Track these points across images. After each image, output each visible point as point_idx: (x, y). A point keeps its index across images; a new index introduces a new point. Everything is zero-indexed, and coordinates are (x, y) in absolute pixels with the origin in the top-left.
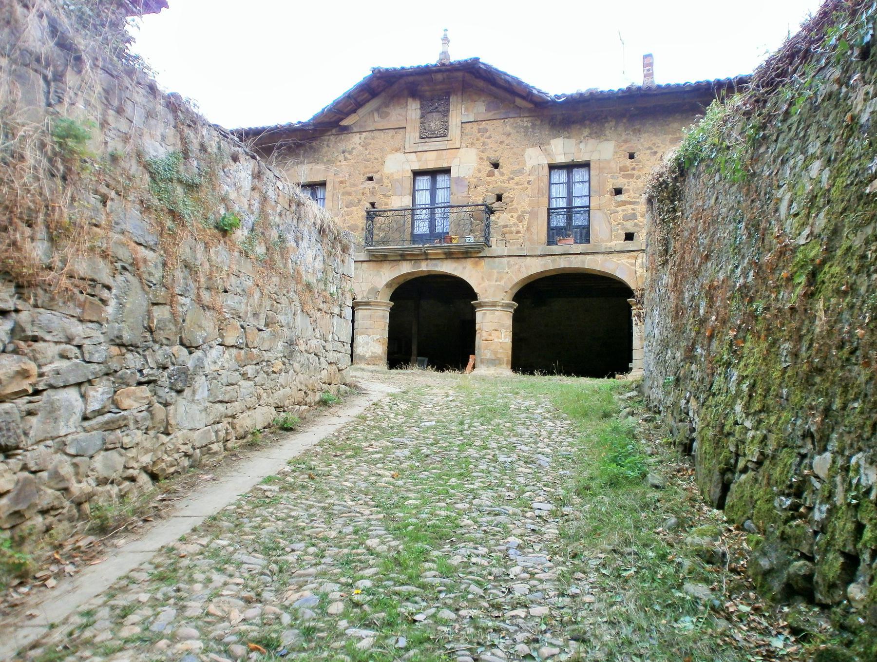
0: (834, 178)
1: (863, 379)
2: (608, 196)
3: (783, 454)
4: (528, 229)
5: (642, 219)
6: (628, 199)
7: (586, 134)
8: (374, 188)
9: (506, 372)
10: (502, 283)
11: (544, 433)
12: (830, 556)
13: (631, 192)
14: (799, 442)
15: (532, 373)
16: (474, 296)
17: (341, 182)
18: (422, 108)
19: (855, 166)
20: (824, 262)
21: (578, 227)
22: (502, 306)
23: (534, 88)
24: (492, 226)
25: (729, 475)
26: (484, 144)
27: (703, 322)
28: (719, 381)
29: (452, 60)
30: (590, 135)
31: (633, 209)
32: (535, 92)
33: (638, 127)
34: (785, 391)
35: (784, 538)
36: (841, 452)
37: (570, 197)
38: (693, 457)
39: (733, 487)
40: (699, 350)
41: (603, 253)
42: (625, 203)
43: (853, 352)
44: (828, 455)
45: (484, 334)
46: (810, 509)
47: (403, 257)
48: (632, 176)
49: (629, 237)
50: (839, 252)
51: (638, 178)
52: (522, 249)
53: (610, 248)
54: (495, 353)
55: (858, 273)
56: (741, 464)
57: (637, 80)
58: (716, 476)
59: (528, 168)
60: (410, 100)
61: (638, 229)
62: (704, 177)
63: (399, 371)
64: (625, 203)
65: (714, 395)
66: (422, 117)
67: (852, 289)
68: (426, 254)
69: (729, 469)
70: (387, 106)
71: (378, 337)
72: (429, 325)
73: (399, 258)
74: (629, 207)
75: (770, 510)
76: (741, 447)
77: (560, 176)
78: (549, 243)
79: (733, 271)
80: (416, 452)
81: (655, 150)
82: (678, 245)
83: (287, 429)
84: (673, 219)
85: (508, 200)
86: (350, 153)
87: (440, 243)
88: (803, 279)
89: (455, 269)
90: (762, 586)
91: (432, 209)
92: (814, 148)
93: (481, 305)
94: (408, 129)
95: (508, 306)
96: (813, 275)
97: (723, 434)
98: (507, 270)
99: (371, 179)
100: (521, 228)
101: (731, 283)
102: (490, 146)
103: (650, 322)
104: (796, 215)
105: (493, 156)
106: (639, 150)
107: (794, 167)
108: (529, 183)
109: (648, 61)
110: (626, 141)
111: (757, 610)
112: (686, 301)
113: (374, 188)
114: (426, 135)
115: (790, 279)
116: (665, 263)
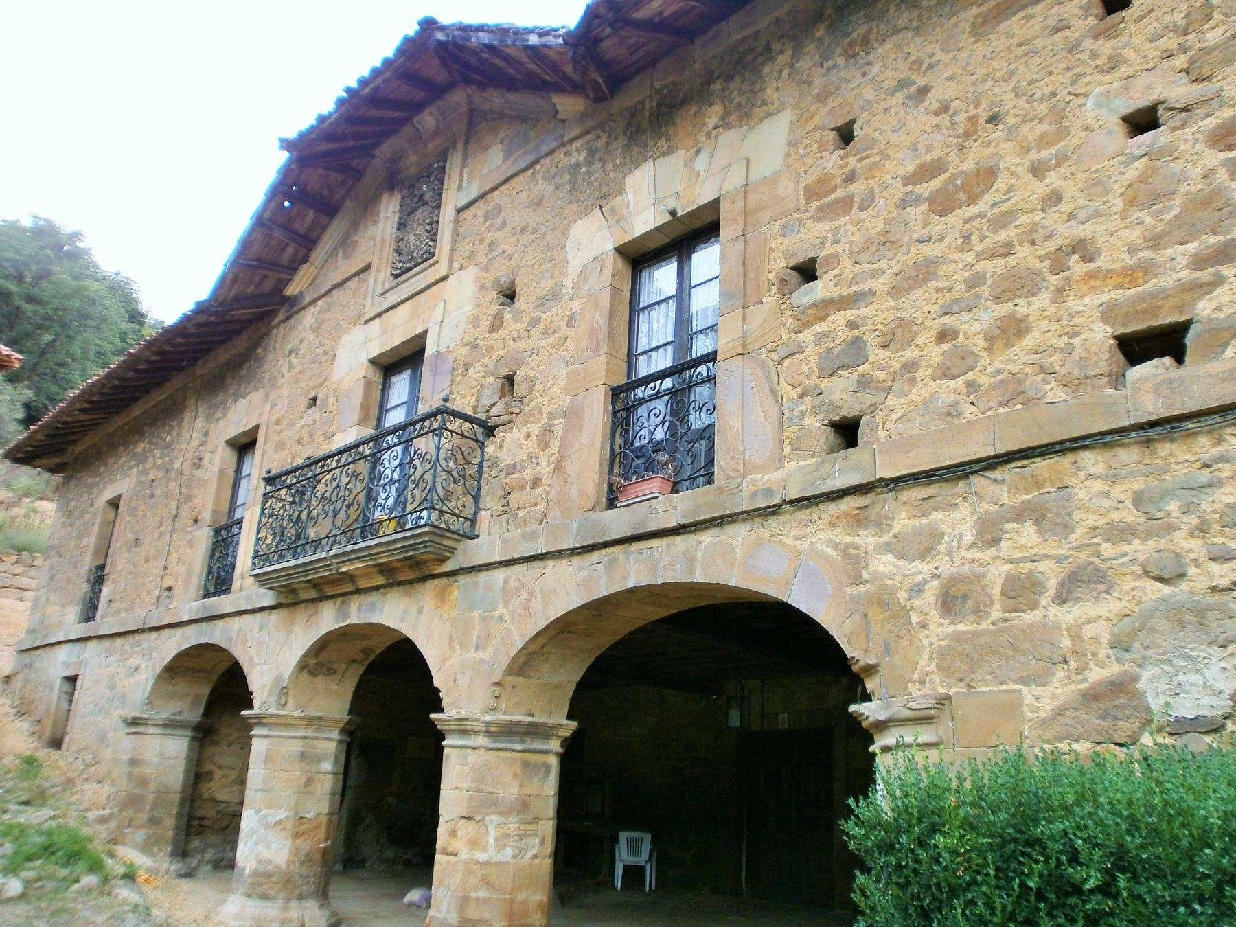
4: (559, 467)
5: (883, 355)
6: (835, 293)
7: (712, 121)
10: (487, 655)
13: (845, 262)
30: (725, 123)
31: (853, 325)
41: (748, 515)
42: (824, 309)
48: (846, 204)
51: (868, 202)
52: (533, 536)
53: (768, 492)
61: (870, 398)
64: (824, 309)
71: (282, 815)
81: (921, 82)
98: (501, 610)
106: (867, 106)
110: (822, 98)
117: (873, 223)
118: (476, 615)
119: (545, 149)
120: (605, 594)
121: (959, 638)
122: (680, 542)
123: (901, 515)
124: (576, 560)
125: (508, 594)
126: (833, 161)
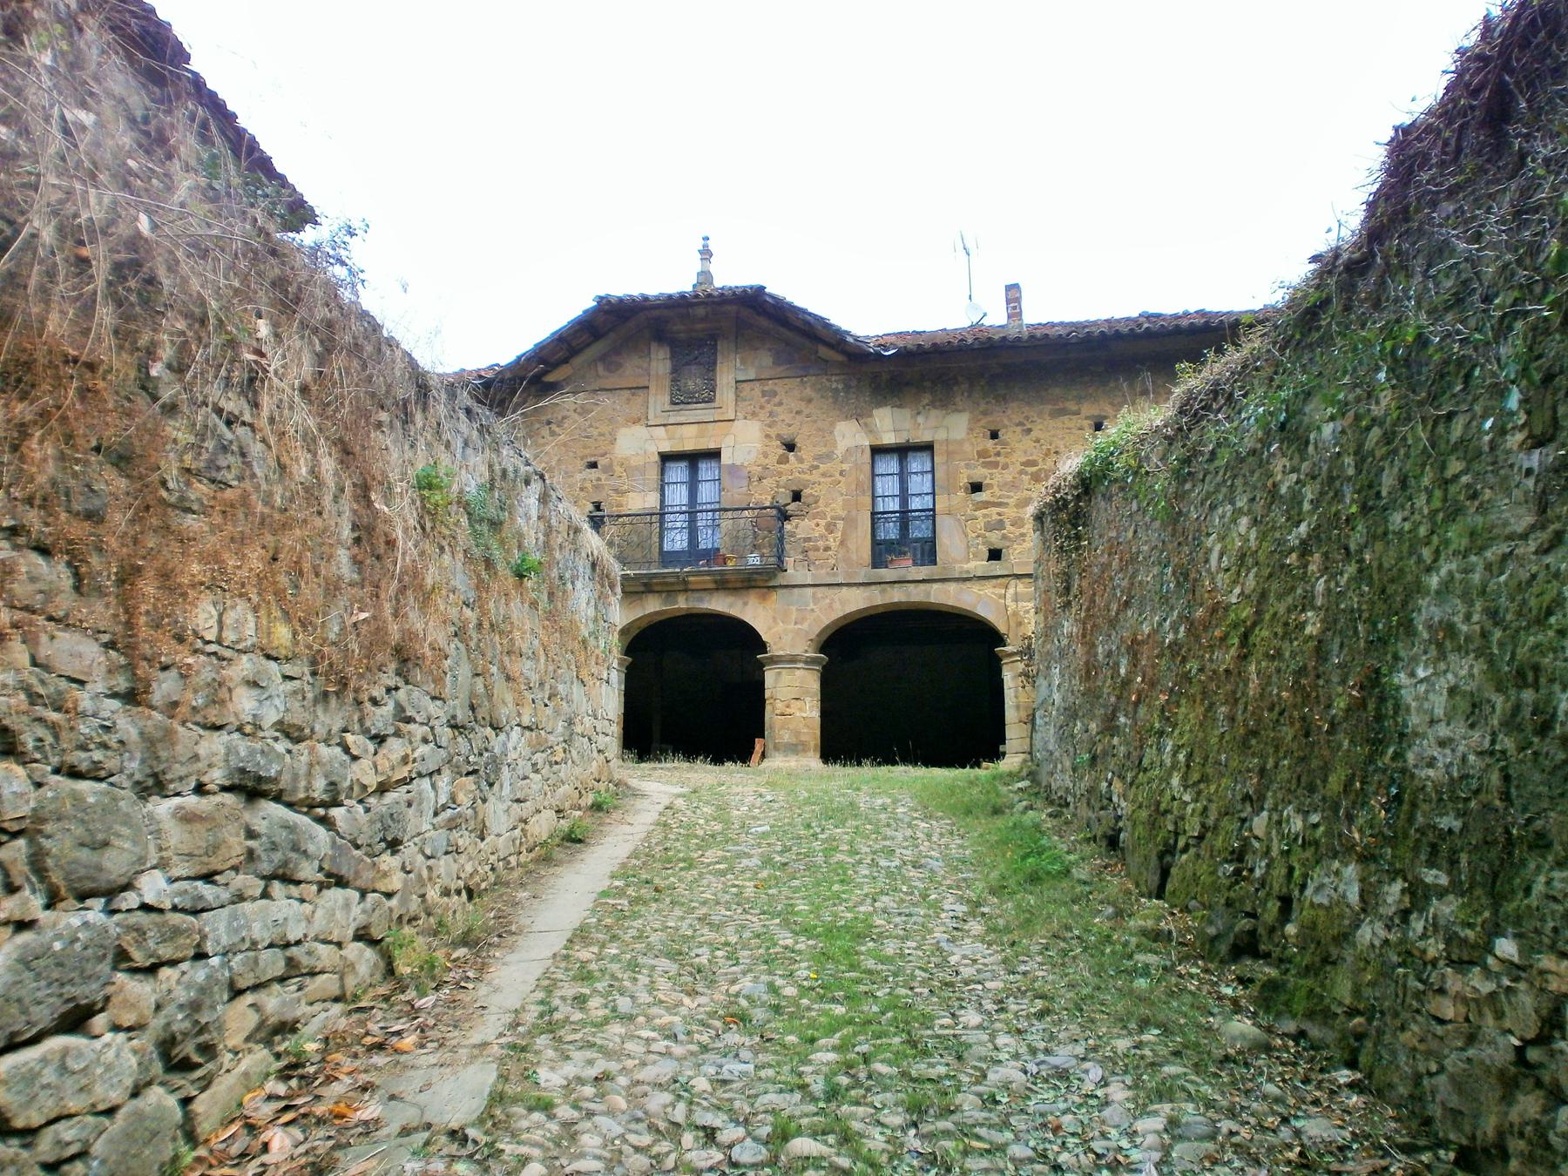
0: (1262, 537)
1: (1290, 737)
2: (961, 494)
3: (1225, 822)
4: (842, 543)
7: (926, 401)
8: (599, 479)
9: (814, 762)
10: (805, 626)
11: (919, 835)
12: (1270, 904)
14: (1239, 807)
15: (859, 764)
16: (762, 646)
18: (672, 358)
19: (1277, 535)
20: (1255, 624)
21: (917, 540)
22: (806, 662)
23: (848, 333)
24: (787, 539)
25: (1168, 858)
26: (771, 414)
27: (1126, 683)
28: (1150, 755)
29: (718, 283)
30: (932, 404)
32: (850, 339)
33: (1002, 392)
34: (1223, 757)
35: (1229, 903)
36: (1275, 809)
37: (904, 496)
38: (1122, 849)
39: (1174, 871)
40: (1122, 720)
43: (1281, 714)
44: (1265, 814)
45: (779, 705)
46: (1252, 870)
48: (995, 465)
49: (995, 555)
50: (1267, 617)
51: (1005, 467)
54: (797, 733)
55: (1282, 639)
56: (1181, 843)
57: (997, 317)
58: (1154, 861)
59: (840, 450)
60: (654, 346)
62: (1117, 499)
63: (657, 765)
65: (1146, 770)
66: (675, 370)
67: (1279, 654)
68: (685, 582)
69: (1169, 850)
72: (689, 693)
73: (642, 589)
74: (995, 510)
75: (1214, 883)
76: (1180, 824)
77: (890, 465)
78: (875, 565)
79: (1160, 624)
80: (767, 861)
82: (1085, 584)
83: (574, 840)
84: (1077, 549)
85: (810, 500)
87: (707, 564)
88: (1236, 641)
89: (731, 606)
90: (1210, 952)
91: (692, 513)
92: (1241, 502)
93: (775, 660)
94: (652, 390)
95: (813, 661)
96: (1245, 638)
97: (1159, 812)
98: (812, 606)
99: (593, 465)
100: (831, 543)
101: (1158, 638)
103: (1045, 683)
104: (1227, 570)
105: (786, 432)
107: (1223, 516)
109: (1013, 294)
110: (985, 413)
111: (1206, 971)
112: (1100, 658)
113: (599, 479)
114: (682, 399)
115: (1223, 639)
116: (1068, 604)
117: (1008, 476)
122: (922, 587)
126: (990, 443)
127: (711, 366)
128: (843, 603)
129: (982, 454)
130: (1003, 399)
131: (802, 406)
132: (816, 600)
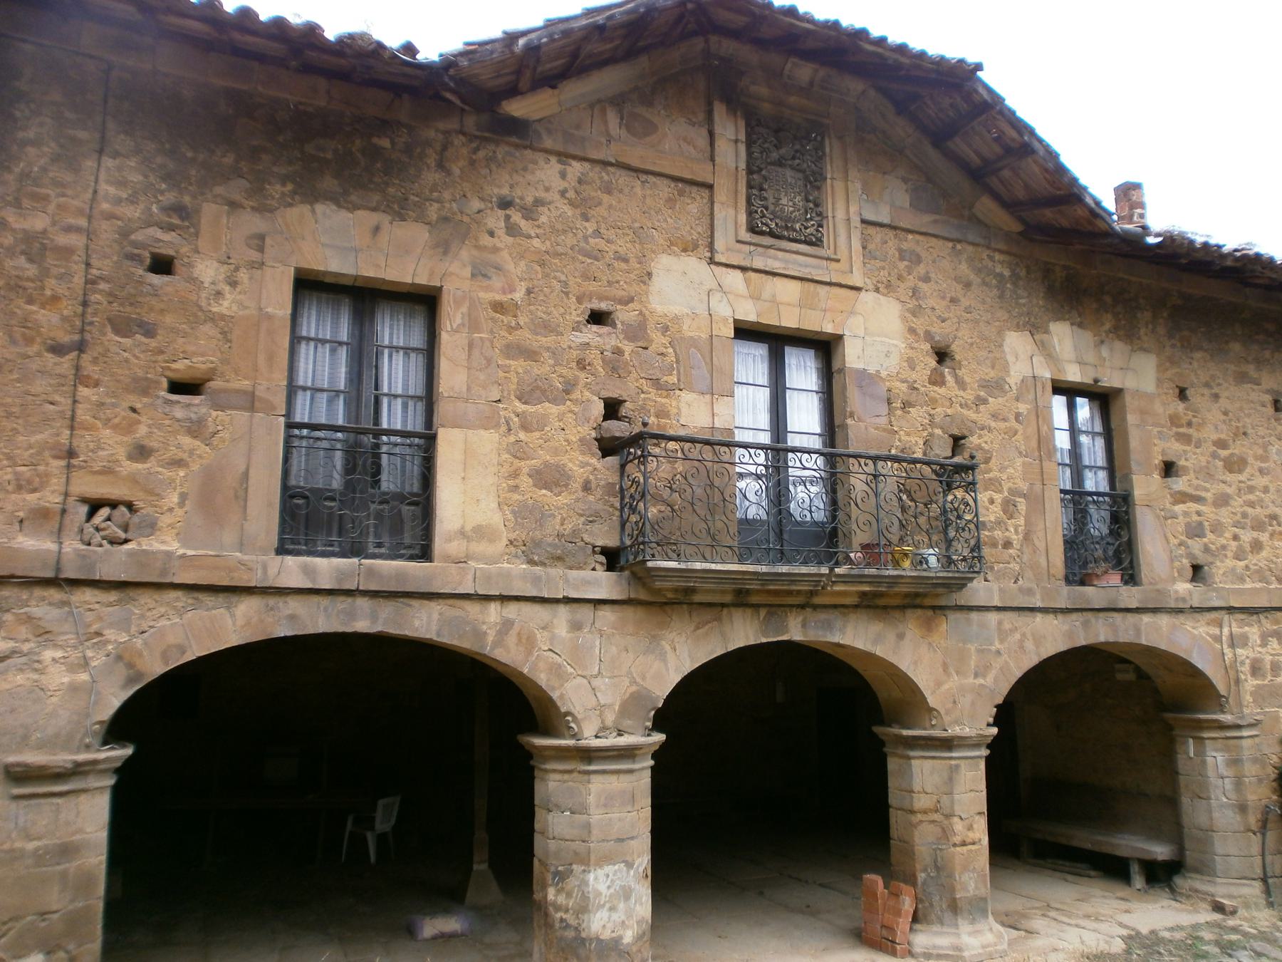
4: (1027, 537)
6: (1191, 491)
10: (989, 680)
17: (498, 307)
26: (915, 292)
42: (1182, 497)
47: (741, 596)
64: (1182, 497)
70: (647, 100)
73: (728, 599)
86: (529, 213)
89: (878, 639)
98: (997, 645)
99: (597, 318)
102: (932, 302)
105: (941, 331)
108: (1018, 416)
113: (618, 352)
118: (972, 647)
119: (971, 237)
120: (1084, 643)
121: (1258, 687)
122: (1131, 618)
123: (1232, 626)
124: (1060, 617)
125: (1003, 635)
126: (1181, 407)
127: (813, 182)
128: (1038, 640)
129: (1174, 420)
130: (1188, 347)
131: (957, 290)
132: (1003, 635)
